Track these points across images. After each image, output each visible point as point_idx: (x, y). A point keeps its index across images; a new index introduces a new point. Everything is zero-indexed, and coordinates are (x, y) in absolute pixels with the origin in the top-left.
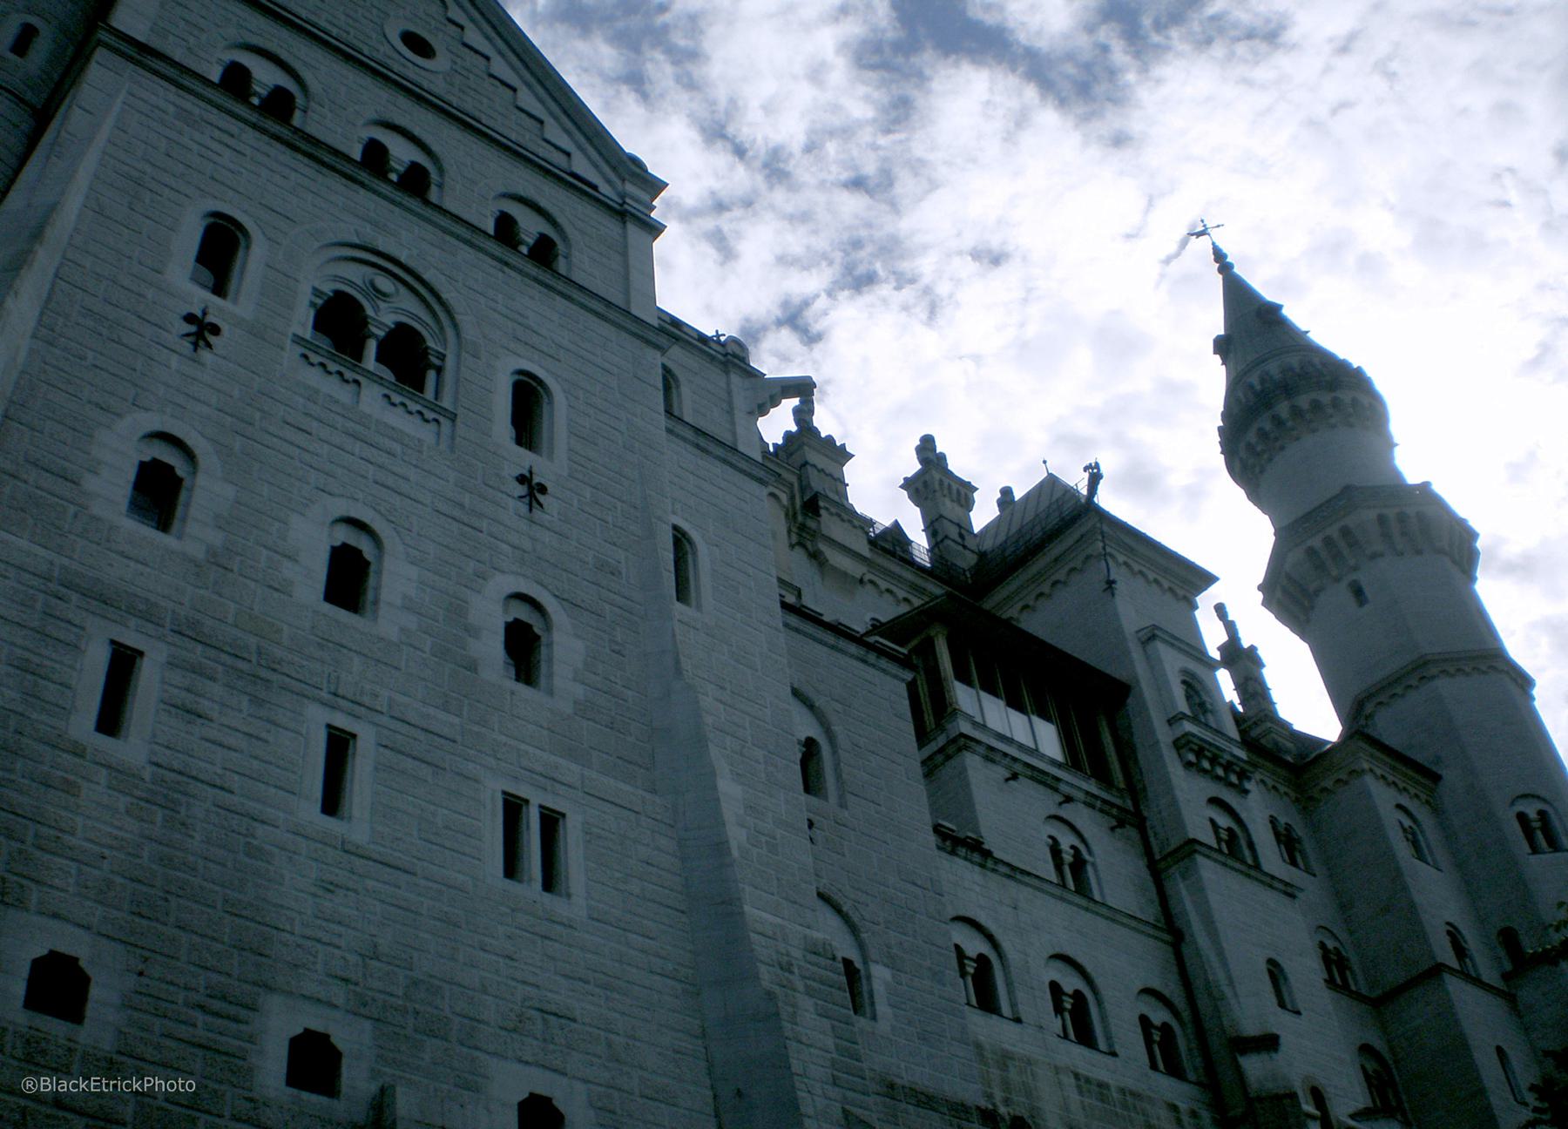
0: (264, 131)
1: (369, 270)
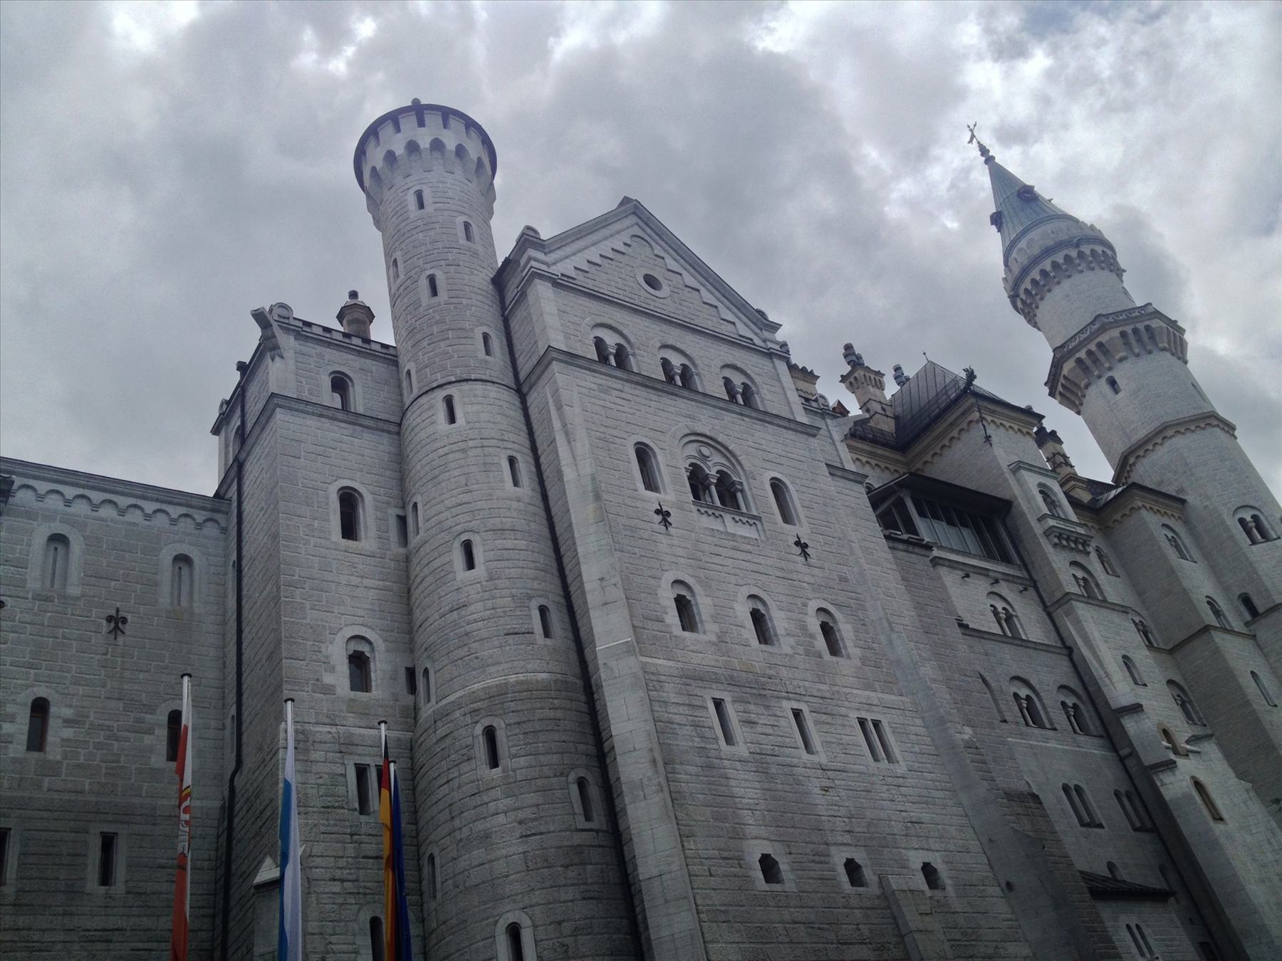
1: (695, 445)
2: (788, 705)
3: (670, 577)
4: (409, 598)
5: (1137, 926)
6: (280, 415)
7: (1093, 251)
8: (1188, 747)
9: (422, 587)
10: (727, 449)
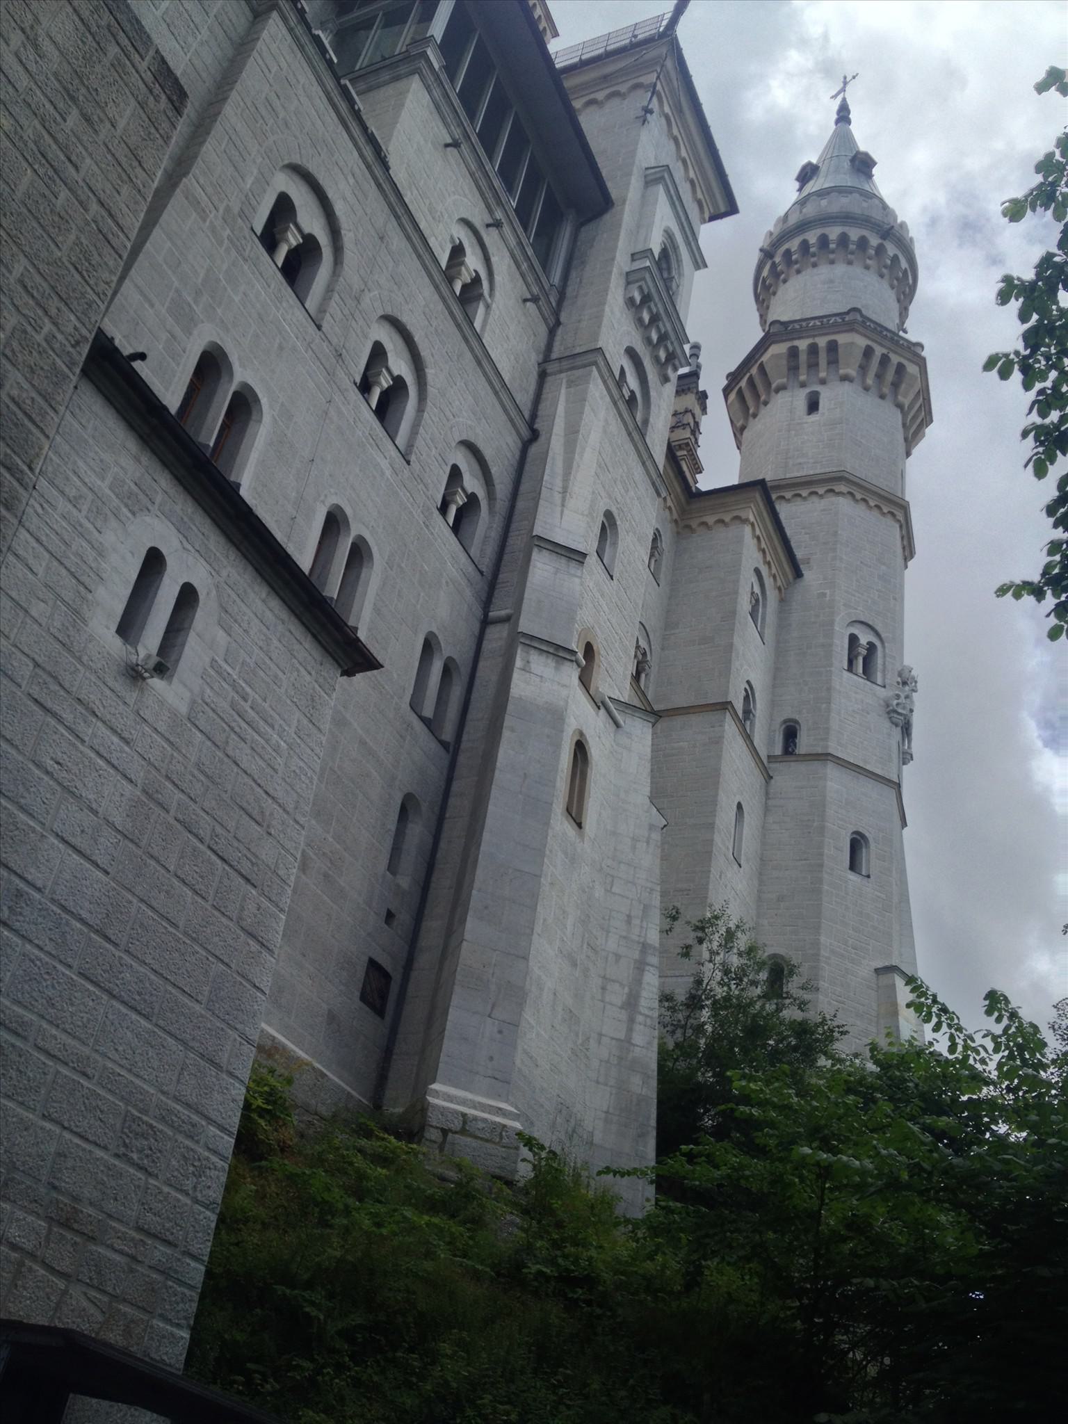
5: (188, 596)
7: (895, 259)
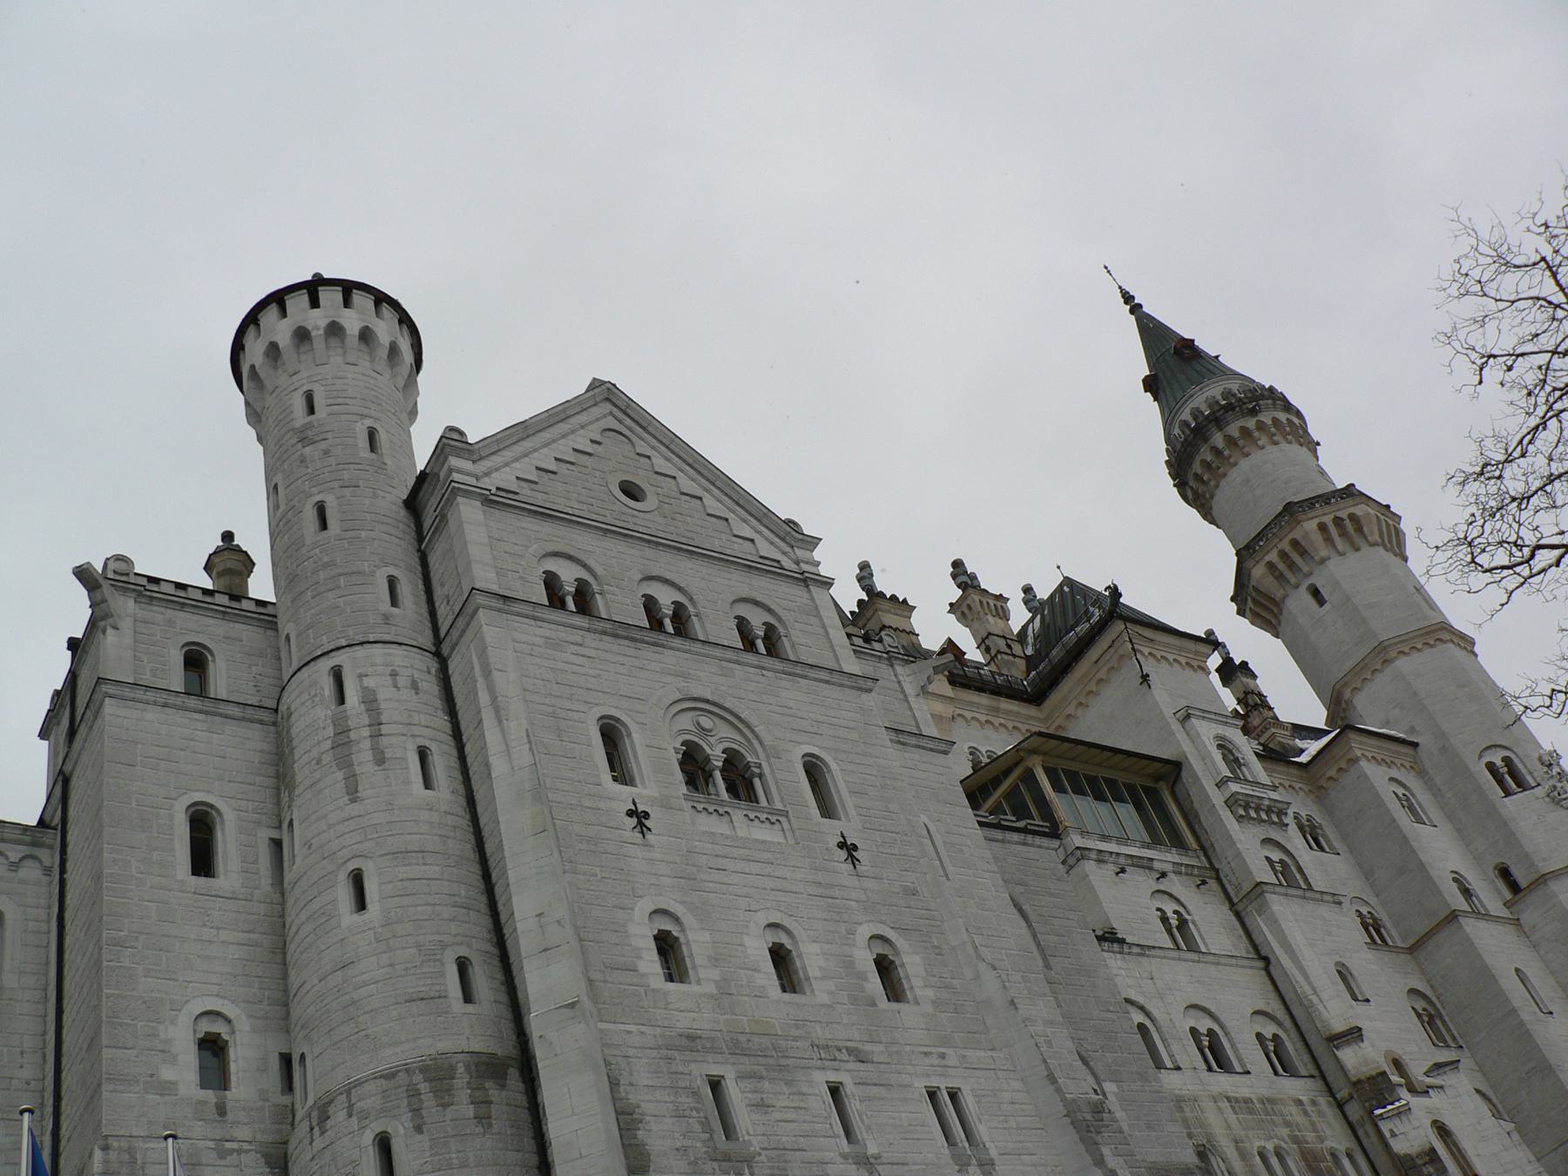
0: (595, 631)
2: (820, 1079)
3: (646, 905)
4: (284, 955)
6: (110, 708)
7: (1275, 420)
8: (1429, 1080)
9: (297, 940)
10: (739, 718)
